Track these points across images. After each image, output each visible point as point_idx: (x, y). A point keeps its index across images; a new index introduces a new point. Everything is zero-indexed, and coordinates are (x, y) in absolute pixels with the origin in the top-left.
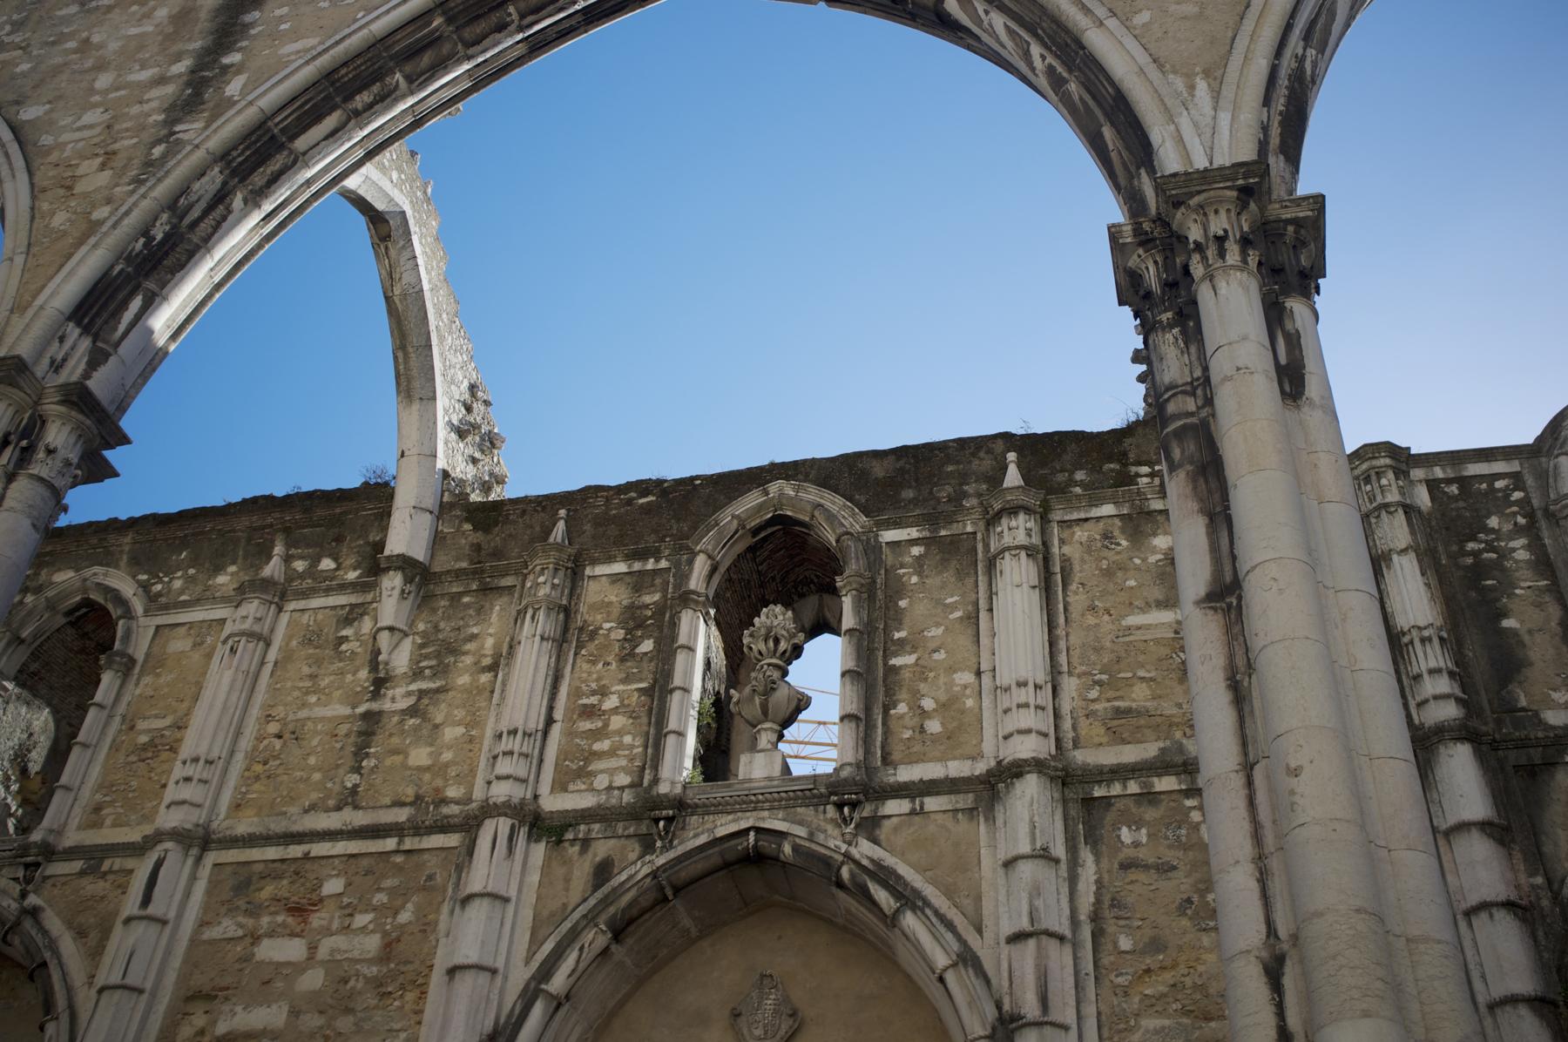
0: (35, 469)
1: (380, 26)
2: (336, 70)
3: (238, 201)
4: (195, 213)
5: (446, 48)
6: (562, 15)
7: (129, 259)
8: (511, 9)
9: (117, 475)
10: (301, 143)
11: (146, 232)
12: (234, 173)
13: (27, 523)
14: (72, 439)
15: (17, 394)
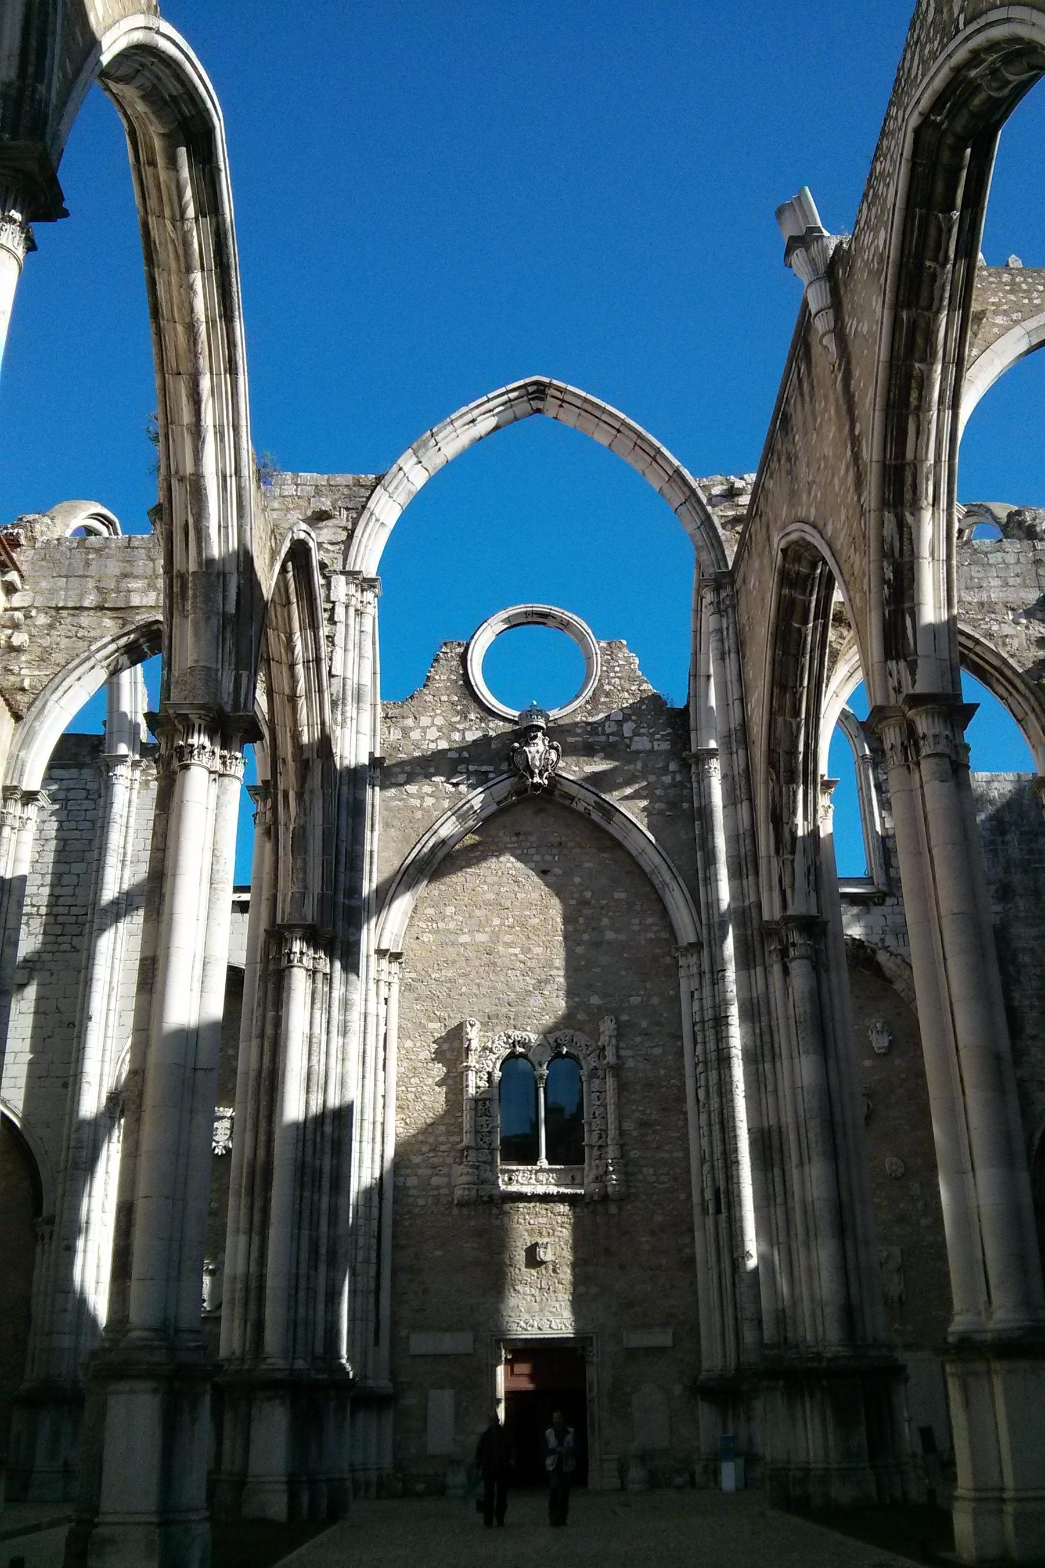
0: (923, 753)
1: (884, 356)
2: (888, 399)
3: (909, 518)
4: (897, 545)
5: (922, 324)
6: (955, 230)
7: (888, 603)
8: (928, 263)
9: (978, 705)
10: (909, 455)
11: (884, 581)
12: (895, 506)
13: (937, 782)
14: (930, 720)
15: (891, 721)
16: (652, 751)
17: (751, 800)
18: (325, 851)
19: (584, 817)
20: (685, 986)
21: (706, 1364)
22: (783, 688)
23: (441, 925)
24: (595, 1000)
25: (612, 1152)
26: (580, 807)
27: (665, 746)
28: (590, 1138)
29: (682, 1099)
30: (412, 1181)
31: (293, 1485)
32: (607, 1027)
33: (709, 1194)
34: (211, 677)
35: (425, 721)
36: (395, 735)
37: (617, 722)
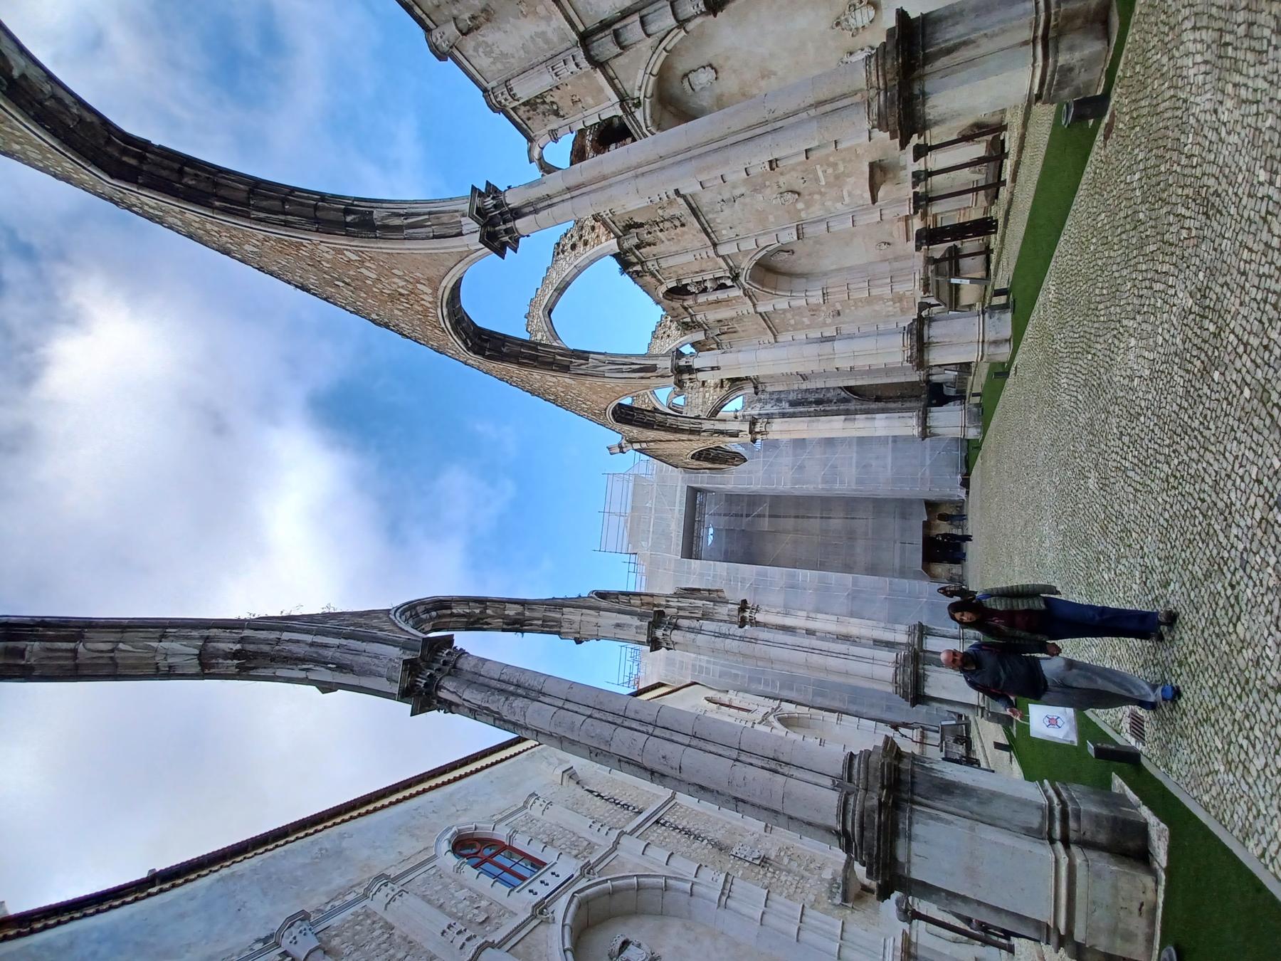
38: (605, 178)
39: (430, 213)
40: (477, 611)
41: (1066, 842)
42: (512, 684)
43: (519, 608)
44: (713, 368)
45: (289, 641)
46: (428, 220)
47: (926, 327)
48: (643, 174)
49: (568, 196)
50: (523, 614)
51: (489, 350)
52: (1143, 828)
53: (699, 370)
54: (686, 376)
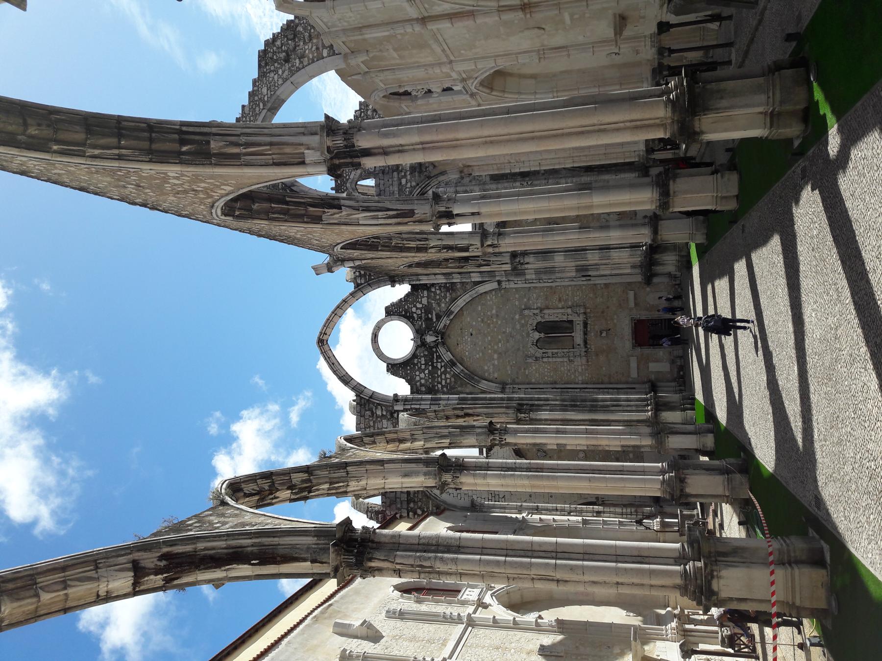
16: (428, 297)
17: (470, 272)
18: (492, 407)
19: (451, 320)
20: (512, 285)
21: (640, 280)
22: (440, 265)
23: (491, 370)
24: (517, 317)
25: (569, 311)
26: (448, 322)
27: (425, 292)
28: (565, 318)
29: (551, 287)
30: (580, 378)
31: (684, 410)
32: (526, 312)
33: (584, 279)
34: (478, 434)
35: (418, 378)
36: (423, 389)
37: (417, 309)
38: (458, 140)
39: (271, 144)
40: (267, 488)
41: (790, 563)
42: (433, 545)
43: (305, 476)
44: (473, 214)
45: (206, 549)
46: (270, 150)
47: (671, 182)
48: (491, 142)
49: (420, 146)
50: (309, 481)
51: (239, 209)
52: (821, 551)
53: (457, 215)
54: (446, 221)
